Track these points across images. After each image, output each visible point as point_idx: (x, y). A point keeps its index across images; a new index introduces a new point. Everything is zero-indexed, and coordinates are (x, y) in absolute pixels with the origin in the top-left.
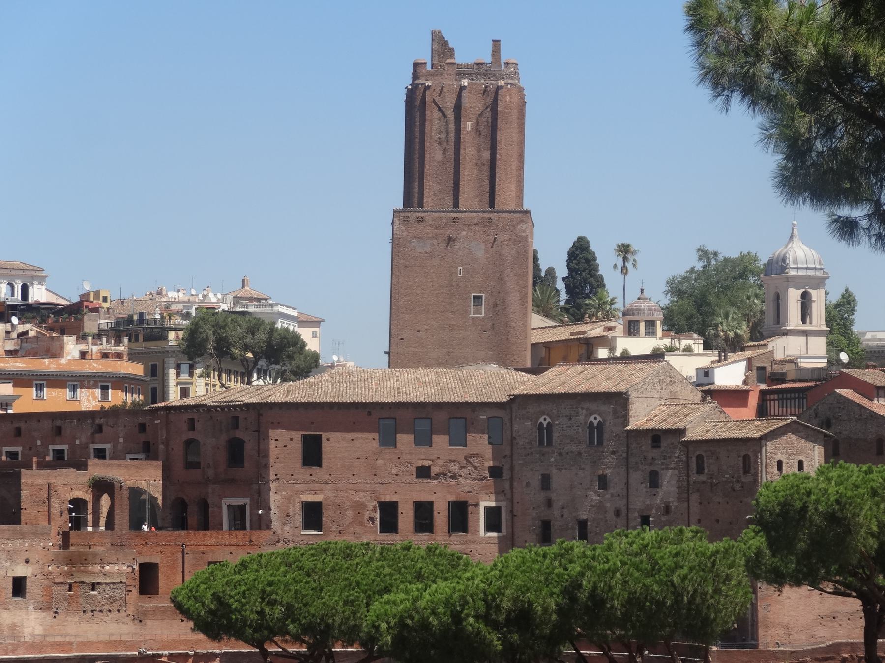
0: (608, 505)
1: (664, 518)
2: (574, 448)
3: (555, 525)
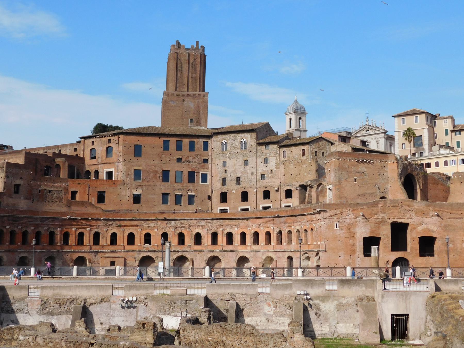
0: (248, 171)
1: (270, 175)
2: (236, 151)
3: (228, 180)
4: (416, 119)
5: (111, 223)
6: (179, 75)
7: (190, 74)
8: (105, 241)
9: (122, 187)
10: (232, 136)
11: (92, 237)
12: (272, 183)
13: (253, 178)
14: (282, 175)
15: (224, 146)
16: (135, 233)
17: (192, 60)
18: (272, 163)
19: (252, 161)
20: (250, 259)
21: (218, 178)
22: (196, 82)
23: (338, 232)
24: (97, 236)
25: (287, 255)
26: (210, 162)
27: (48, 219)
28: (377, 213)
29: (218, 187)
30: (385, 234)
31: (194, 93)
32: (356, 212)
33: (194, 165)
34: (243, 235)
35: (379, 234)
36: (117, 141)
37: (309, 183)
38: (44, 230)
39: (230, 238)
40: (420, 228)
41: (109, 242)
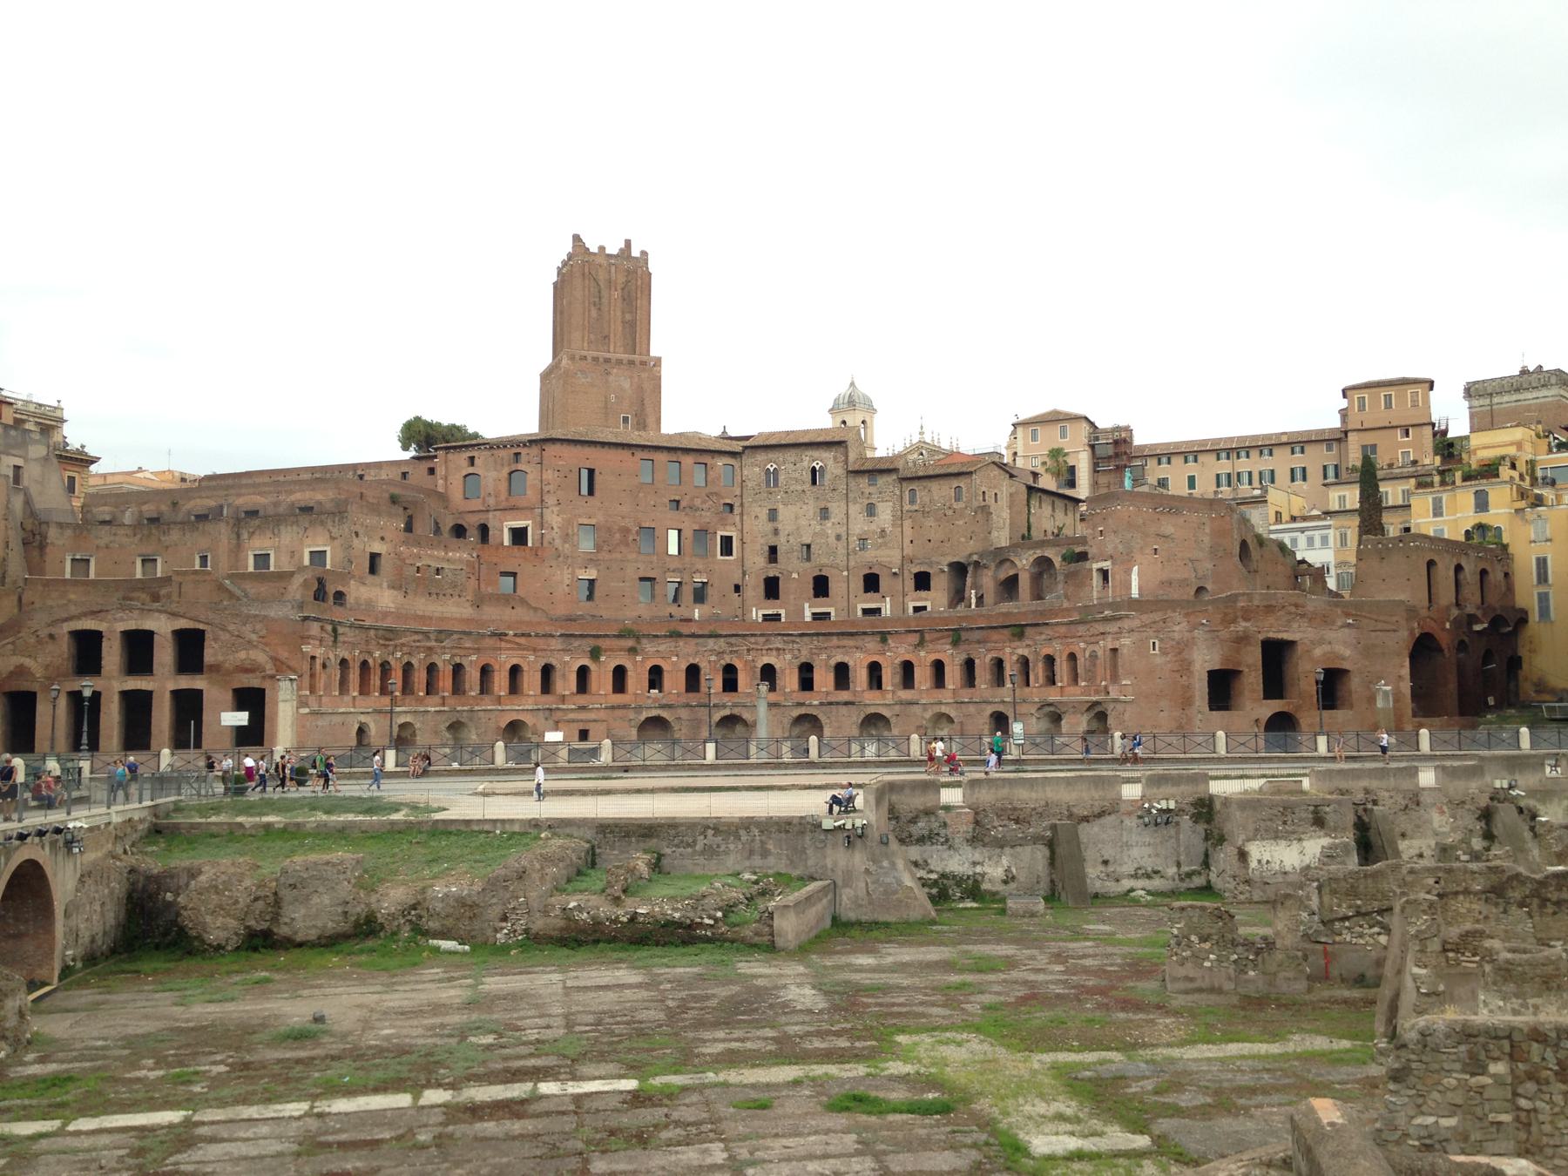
2: (799, 488)
4: (1063, 429)
5: (576, 643)
8: (566, 683)
9: (554, 563)
10: (791, 455)
12: (887, 557)
13: (841, 546)
14: (907, 541)
15: (772, 477)
16: (629, 666)
18: (885, 513)
19: (837, 509)
20: (893, 721)
21: (758, 547)
23: (1159, 660)
24: (547, 671)
25: (990, 710)
26: (737, 510)
27: (450, 633)
28: (1234, 621)
29: (757, 563)
30: (1251, 662)
31: (632, 357)
32: (1192, 618)
33: (707, 517)
34: (875, 670)
35: (1239, 664)
36: (537, 459)
37: (975, 558)
38: (443, 661)
39: (842, 674)
40: (1318, 652)
41: (574, 689)
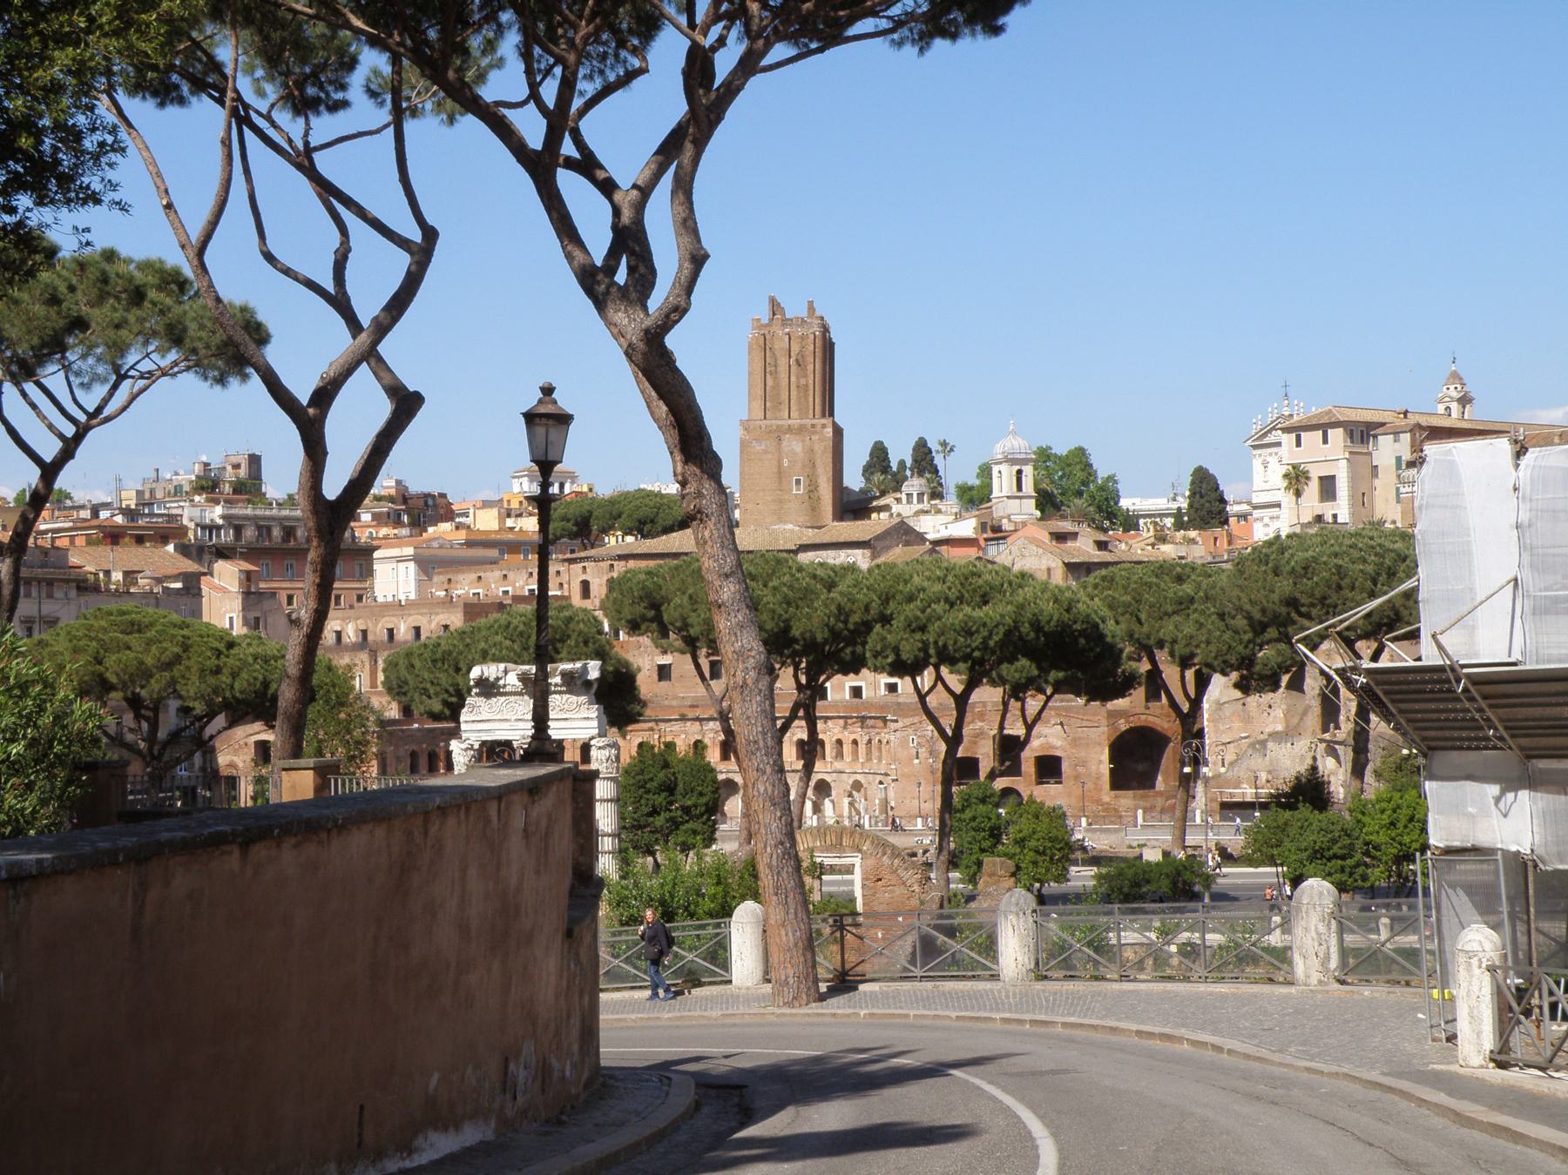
6: (770, 382)
7: (793, 379)
11: (578, 752)
17: (795, 349)
22: (806, 397)
